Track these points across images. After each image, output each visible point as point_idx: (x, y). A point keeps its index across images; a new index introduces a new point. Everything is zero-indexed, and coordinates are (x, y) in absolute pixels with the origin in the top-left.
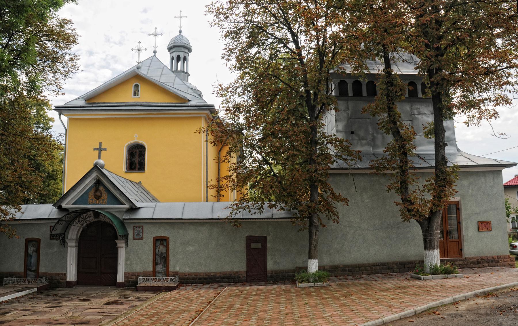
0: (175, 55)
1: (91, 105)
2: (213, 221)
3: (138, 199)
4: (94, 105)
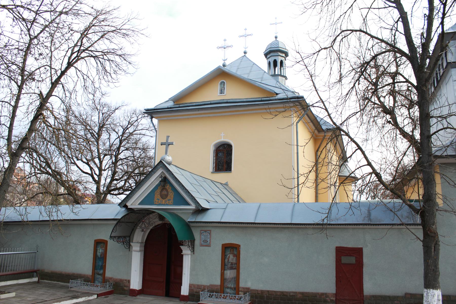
0: (272, 59)
1: (178, 106)
2: (293, 226)
3: (209, 198)
4: (180, 106)
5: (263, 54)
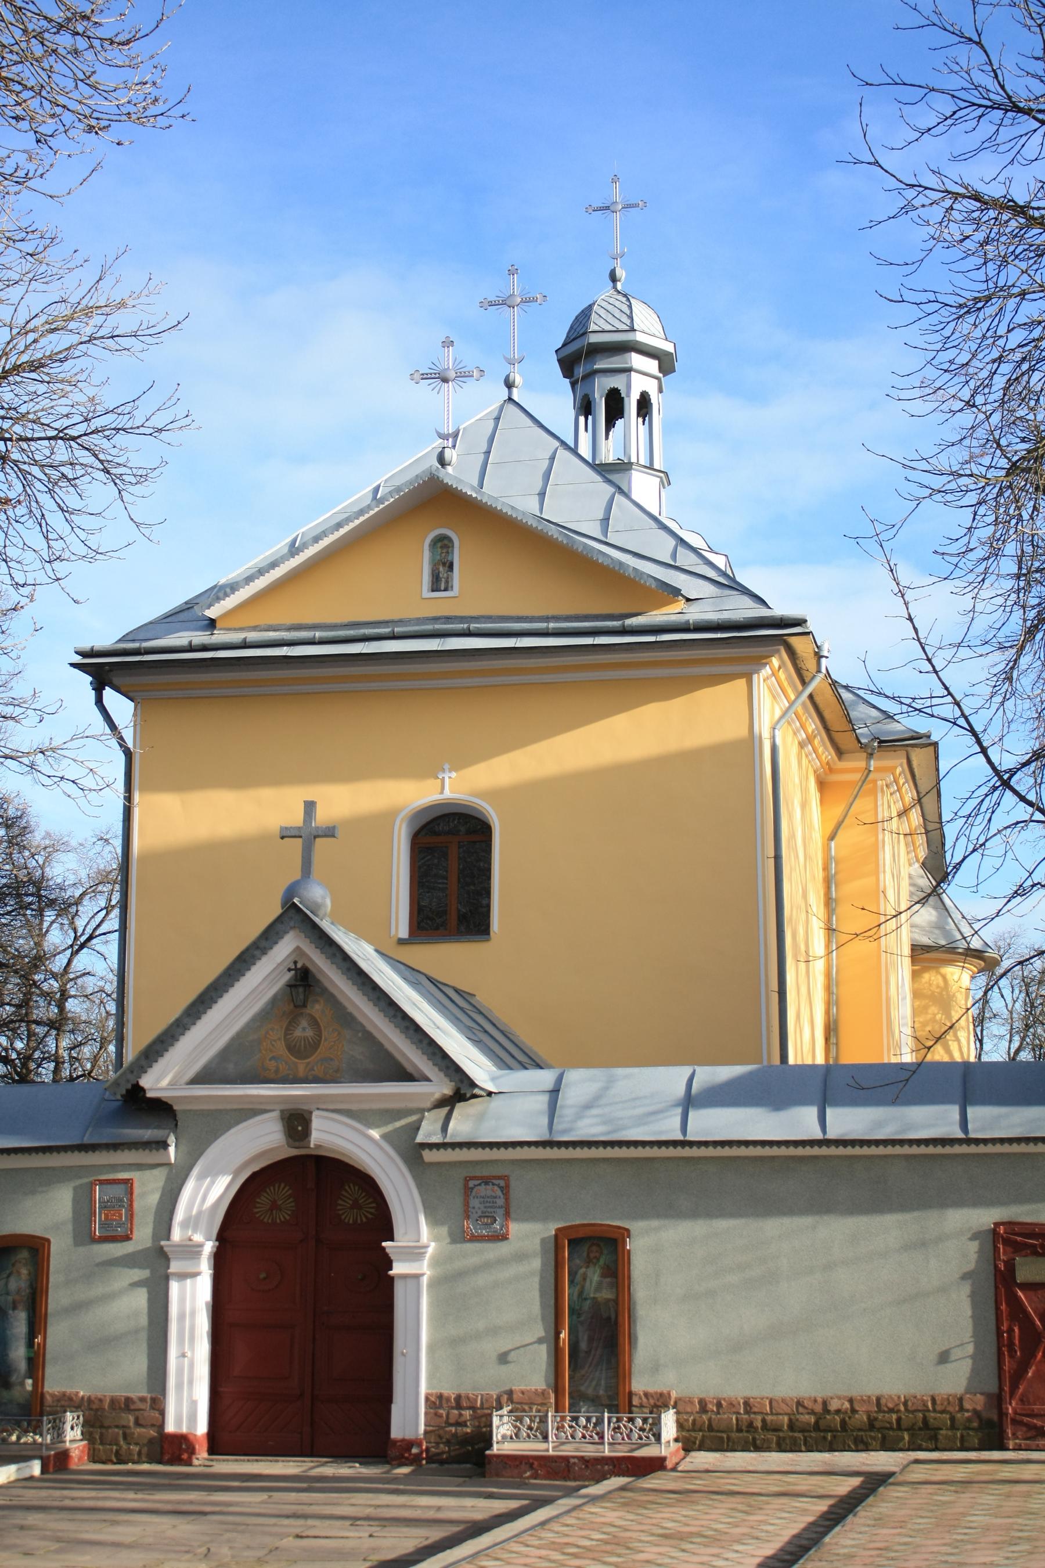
5: (554, 358)
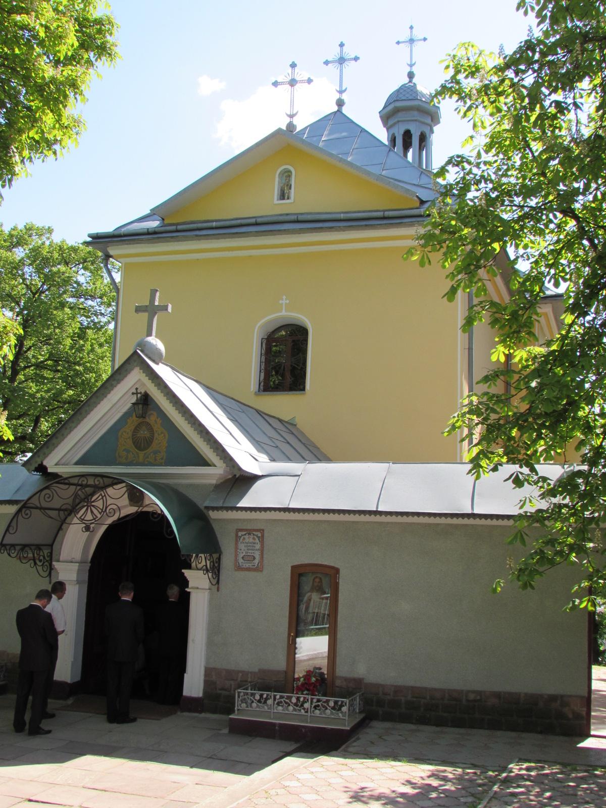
0: (399, 132)
1: (173, 228)
4: (180, 227)
5: (378, 115)
